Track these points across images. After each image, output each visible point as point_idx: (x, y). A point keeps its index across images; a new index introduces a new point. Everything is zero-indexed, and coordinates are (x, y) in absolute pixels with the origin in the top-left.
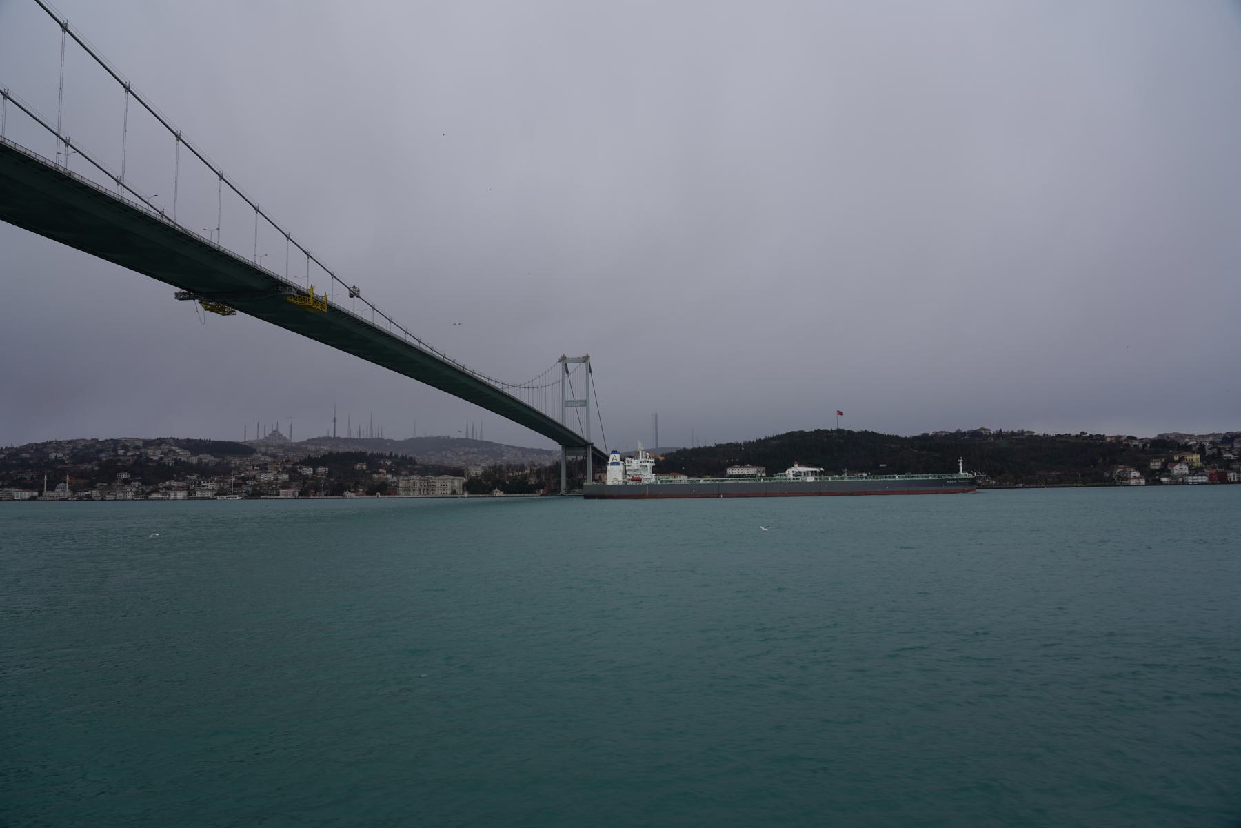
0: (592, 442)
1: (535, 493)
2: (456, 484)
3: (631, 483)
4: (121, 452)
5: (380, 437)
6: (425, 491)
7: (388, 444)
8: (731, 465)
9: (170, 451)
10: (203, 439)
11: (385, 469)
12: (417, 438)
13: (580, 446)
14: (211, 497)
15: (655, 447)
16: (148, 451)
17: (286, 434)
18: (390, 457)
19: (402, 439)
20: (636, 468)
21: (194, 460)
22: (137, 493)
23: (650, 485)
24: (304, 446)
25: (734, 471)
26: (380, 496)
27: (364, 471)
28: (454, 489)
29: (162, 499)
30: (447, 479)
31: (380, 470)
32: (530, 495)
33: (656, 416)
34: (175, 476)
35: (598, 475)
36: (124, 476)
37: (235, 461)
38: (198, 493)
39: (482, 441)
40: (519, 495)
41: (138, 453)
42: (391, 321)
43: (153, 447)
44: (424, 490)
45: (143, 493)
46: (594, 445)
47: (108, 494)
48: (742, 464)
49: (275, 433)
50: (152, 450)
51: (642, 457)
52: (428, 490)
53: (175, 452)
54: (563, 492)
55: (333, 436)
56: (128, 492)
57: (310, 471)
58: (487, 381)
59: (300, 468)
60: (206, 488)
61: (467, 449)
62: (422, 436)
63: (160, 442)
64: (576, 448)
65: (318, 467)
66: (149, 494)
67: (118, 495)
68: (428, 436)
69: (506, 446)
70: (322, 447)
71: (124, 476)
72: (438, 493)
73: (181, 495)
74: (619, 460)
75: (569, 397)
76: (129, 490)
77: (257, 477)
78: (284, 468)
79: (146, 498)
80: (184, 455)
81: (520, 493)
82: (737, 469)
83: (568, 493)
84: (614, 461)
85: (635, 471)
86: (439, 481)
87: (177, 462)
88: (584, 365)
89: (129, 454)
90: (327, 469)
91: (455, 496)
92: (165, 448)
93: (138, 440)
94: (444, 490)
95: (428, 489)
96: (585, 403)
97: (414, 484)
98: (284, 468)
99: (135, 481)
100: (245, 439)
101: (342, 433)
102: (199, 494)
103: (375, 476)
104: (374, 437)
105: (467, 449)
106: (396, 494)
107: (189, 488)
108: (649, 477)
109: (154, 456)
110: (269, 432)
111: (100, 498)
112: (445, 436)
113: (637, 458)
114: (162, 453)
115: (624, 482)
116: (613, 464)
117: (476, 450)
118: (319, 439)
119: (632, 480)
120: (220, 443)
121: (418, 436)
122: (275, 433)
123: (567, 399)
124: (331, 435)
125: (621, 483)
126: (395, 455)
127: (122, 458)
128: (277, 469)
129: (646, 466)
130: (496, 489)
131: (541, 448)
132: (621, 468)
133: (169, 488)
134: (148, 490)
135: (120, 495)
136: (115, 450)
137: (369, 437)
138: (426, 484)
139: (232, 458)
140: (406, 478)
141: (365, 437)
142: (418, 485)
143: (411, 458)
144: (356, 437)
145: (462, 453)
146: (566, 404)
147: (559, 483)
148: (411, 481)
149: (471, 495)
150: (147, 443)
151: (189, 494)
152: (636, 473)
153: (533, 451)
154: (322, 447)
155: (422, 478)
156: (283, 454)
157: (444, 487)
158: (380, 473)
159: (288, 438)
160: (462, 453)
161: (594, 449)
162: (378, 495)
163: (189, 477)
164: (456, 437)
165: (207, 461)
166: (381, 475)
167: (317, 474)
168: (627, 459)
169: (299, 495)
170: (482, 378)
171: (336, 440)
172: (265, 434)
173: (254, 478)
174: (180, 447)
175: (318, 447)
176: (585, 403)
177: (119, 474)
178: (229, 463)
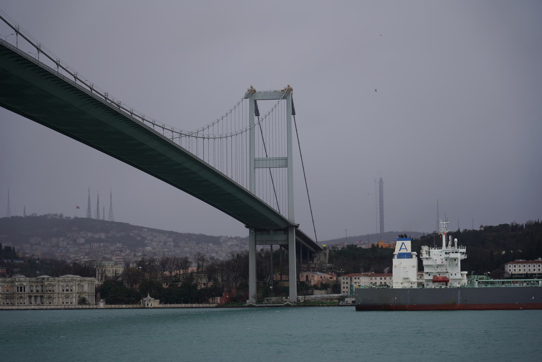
0: (296, 223)
2: (86, 288)
3: (432, 286)
6: (39, 299)
8: (512, 259)
13: (278, 229)
15: (379, 232)
20: (439, 262)
23: (462, 289)
25: (517, 268)
30: (72, 280)
32: (201, 305)
33: (381, 181)
35: (305, 274)
39: (113, 222)
40: (183, 305)
42: (17, 32)
46: (300, 228)
51: (447, 246)
52: (42, 297)
54: (251, 300)
58: (151, 126)
61: (90, 235)
64: (272, 232)
68: (28, 214)
69: (149, 230)
72: (58, 302)
74: (409, 250)
75: (259, 153)
81: (186, 302)
82: (522, 266)
83: (258, 302)
84: (403, 251)
85: (438, 266)
88: (284, 103)
91: (84, 306)
94: (67, 297)
96: (285, 162)
97: (21, 289)
105: (90, 235)
108: (459, 276)
112: (56, 215)
113: (440, 246)
115: (419, 284)
116: (401, 256)
117: (103, 236)
119: (434, 281)
121: (14, 214)
123: (257, 157)
125: (415, 286)
129: (455, 259)
130: (149, 297)
131: (507, 223)
132: (414, 261)
138: (39, 288)
142: (27, 290)
143: (8, 249)
145: (82, 241)
146: (255, 163)
147: (246, 287)
148: (17, 284)
149: (110, 306)
152: (439, 270)
153: (189, 237)
155: (34, 279)
160: (82, 241)
161: (300, 234)
164: (72, 217)
168: (425, 248)
170: (145, 122)
176: (285, 162)
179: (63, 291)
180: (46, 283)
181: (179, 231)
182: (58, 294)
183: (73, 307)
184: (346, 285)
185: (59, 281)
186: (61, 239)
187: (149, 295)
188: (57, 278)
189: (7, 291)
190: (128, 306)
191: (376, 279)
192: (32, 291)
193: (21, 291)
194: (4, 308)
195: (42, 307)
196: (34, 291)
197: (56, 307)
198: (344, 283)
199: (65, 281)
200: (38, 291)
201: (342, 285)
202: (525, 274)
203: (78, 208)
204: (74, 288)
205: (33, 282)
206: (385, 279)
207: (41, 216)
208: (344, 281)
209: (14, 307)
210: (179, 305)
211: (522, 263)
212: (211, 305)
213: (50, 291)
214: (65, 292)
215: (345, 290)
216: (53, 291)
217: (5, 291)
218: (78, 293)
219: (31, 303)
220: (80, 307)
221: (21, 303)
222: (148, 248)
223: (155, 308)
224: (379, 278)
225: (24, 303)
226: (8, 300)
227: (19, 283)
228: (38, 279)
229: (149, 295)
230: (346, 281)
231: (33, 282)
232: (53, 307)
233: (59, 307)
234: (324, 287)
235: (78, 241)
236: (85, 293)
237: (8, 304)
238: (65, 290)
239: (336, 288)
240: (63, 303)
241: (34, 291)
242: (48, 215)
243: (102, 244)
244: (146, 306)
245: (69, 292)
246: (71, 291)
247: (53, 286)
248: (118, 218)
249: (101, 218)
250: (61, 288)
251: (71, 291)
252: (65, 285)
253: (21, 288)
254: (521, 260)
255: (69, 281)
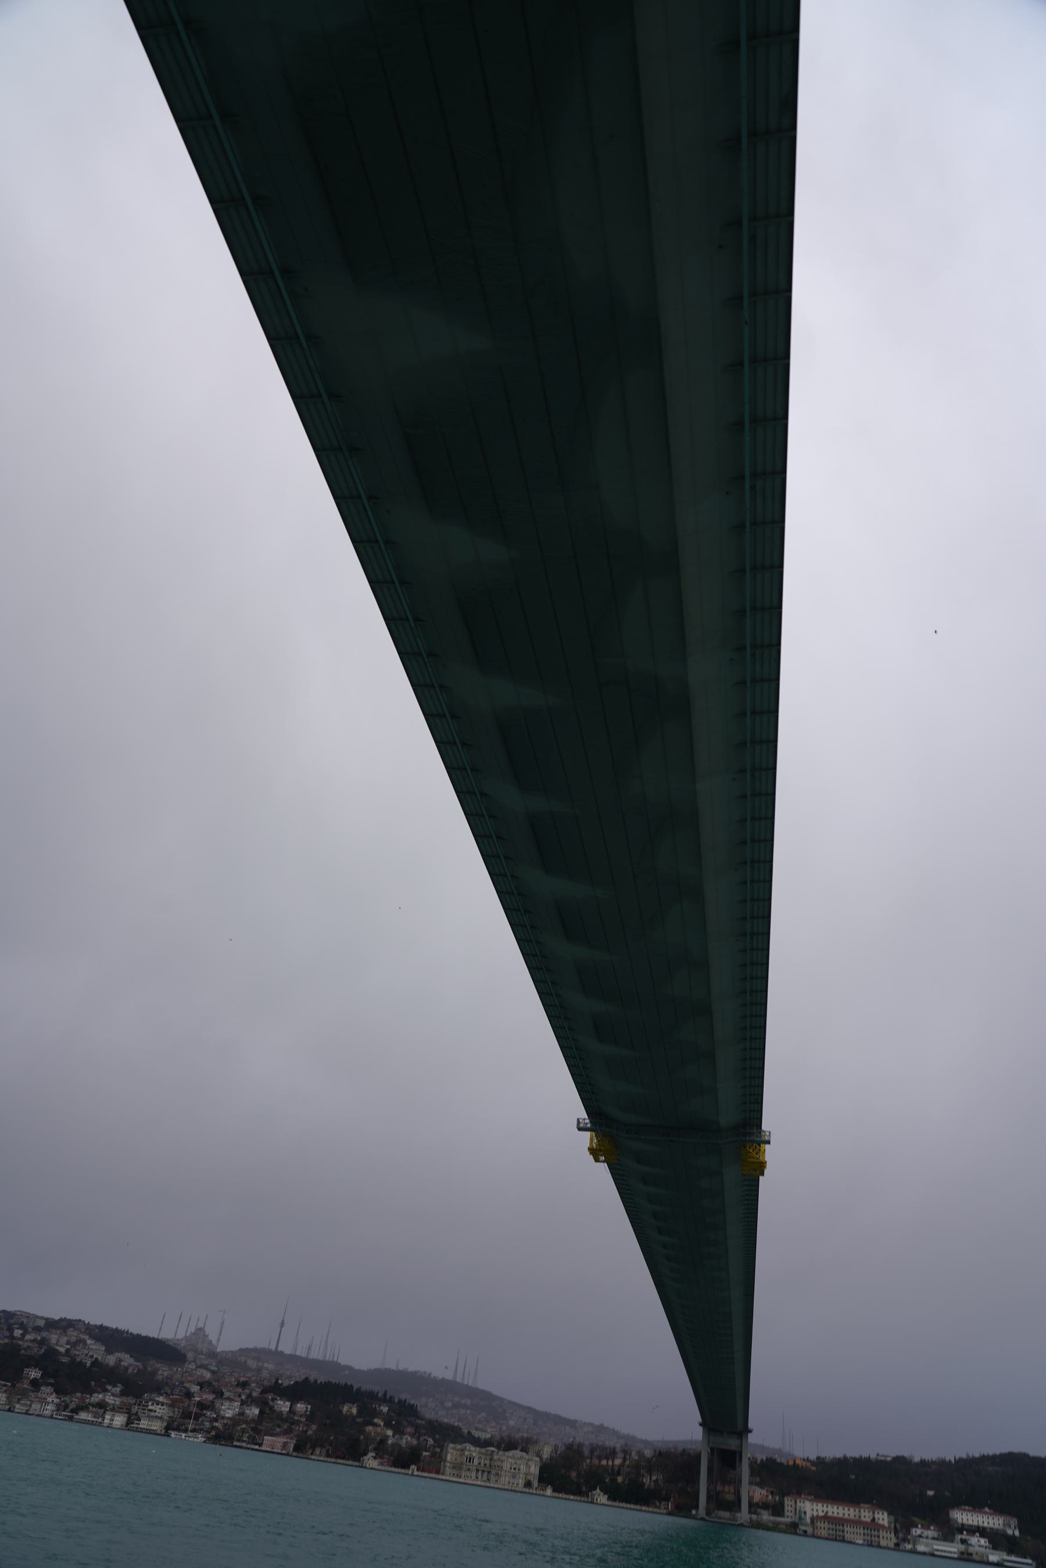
1: (656, 1507)
4: (18, 1333)
5: (335, 1360)
6: (486, 1474)
7: (347, 1372)
9: (80, 1341)
10: (119, 1328)
11: (383, 1419)
12: (386, 1369)
14: (158, 1432)
16: (53, 1336)
17: (213, 1337)
18: (386, 1400)
19: (364, 1368)
21: (111, 1360)
22: (59, 1408)
24: (243, 1359)
25: (965, 1517)
26: (416, 1473)
27: (354, 1418)
28: (529, 1478)
29: (92, 1423)
30: (521, 1458)
31: (376, 1420)
34: (93, 1383)
36: (34, 1374)
37: (163, 1371)
38: (142, 1422)
39: (477, 1389)
41: (39, 1338)
43: (58, 1332)
44: (483, 1471)
45: (66, 1407)
47: (18, 1402)
48: (976, 1506)
49: (200, 1331)
50: (56, 1336)
52: (489, 1472)
53: (84, 1342)
55: (274, 1349)
56: (49, 1403)
57: (286, 1407)
59: (273, 1400)
60: (152, 1414)
61: (456, 1399)
62: (394, 1367)
63: (65, 1325)
65: (298, 1402)
66: (76, 1411)
67: (34, 1406)
68: (401, 1368)
69: (510, 1402)
70: (266, 1365)
71: (34, 1374)
72: (505, 1480)
73: (119, 1420)
76: (49, 1400)
77: (217, 1405)
78: (249, 1396)
79: (71, 1419)
80: (96, 1350)
81: (636, 1503)
82: (970, 1515)
86: (509, 1460)
87: (96, 1363)
89: (28, 1337)
90: (309, 1407)
92: (73, 1336)
93: (42, 1318)
94: (514, 1477)
95: (489, 1471)
97: (470, 1459)
98: (249, 1396)
99: (48, 1384)
100: (175, 1336)
101: (286, 1348)
102: (144, 1424)
103: (369, 1428)
104: (327, 1359)
106: (438, 1472)
107: (130, 1410)
109: (57, 1344)
110: (192, 1329)
111: (8, 1407)
112: (425, 1373)
114: (68, 1343)
118: (255, 1350)
120: (139, 1336)
122: (200, 1331)
124: (273, 1347)
126: (391, 1397)
127: (21, 1343)
128: (240, 1396)
133: (102, 1406)
134: (72, 1406)
135: (36, 1406)
136: (10, 1329)
137: (320, 1358)
138: (488, 1462)
139: (160, 1365)
140: (459, 1447)
141: (315, 1358)
142: (476, 1462)
144: (304, 1355)
149: (557, 1495)
150: (51, 1325)
151: (129, 1422)
153: (546, 1416)
154: (266, 1365)
155: (483, 1450)
156: (216, 1369)
157: (515, 1473)
158: (376, 1425)
159: (214, 1342)
160: (449, 1404)
162: (413, 1470)
163: (109, 1388)
165: (126, 1364)
166: (379, 1429)
167: (294, 1414)
169: (295, 1450)
171: (277, 1355)
172: (187, 1332)
173: (211, 1406)
174: (92, 1337)
175: (260, 1364)
177: (26, 1371)
178: (154, 1373)
179: (511, 1468)
180: (495, 1457)
181: (538, 1408)
182: (506, 1472)
183: (520, 1490)
184: (789, 1508)
185: (508, 1457)
186: (431, 1399)
187: (598, 1488)
188: (506, 1453)
189: (456, 1460)
190: (576, 1498)
191: (817, 1505)
192: (480, 1464)
193: (470, 1462)
194: (452, 1479)
195: (488, 1484)
196: (482, 1464)
197: (502, 1487)
198: (788, 1505)
199: (513, 1457)
200: (485, 1465)
201: (786, 1508)
202: (975, 1526)
203: (446, 1368)
204: (522, 1467)
205: (481, 1453)
206: (827, 1507)
207: (411, 1372)
208: (788, 1502)
209: (461, 1480)
210: (629, 1506)
211: (969, 1511)
212: (662, 1511)
213: (498, 1466)
214: (512, 1470)
215: (789, 1514)
216: (502, 1467)
217: (454, 1459)
218: (526, 1474)
219: (477, 1478)
220: (527, 1490)
221: (468, 1477)
222: (512, 1423)
223: (602, 1504)
224: (842, 1508)
225: (471, 1477)
226: (454, 1470)
227: (468, 1453)
228: (487, 1451)
229: (598, 1488)
230: (790, 1503)
231: (481, 1453)
232: (500, 1486)
233: (506, 1487)
234: (765, 1506)
235: (445, 1404)
236: (531, 1474)
237: (454, 1475)
238: (513, 1468)
239: (778, 1510)
240: (509, 1483)
241: (482, 1464)
242: (418, 1372)
243: (468, 1412)
244: (595, 1501)
245: (517, 1471)
246: (519, 1470)
247: (502, 1461)
248: (481, 1386)
249: (466, 1383)
250: (509, 1464)
251: (519, 1470)
252: (513, 1463)
253: (470, 1459)
254: (967, 1508)
255: (518, 1459)
